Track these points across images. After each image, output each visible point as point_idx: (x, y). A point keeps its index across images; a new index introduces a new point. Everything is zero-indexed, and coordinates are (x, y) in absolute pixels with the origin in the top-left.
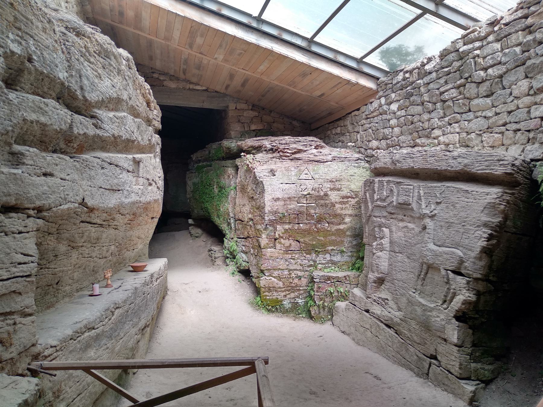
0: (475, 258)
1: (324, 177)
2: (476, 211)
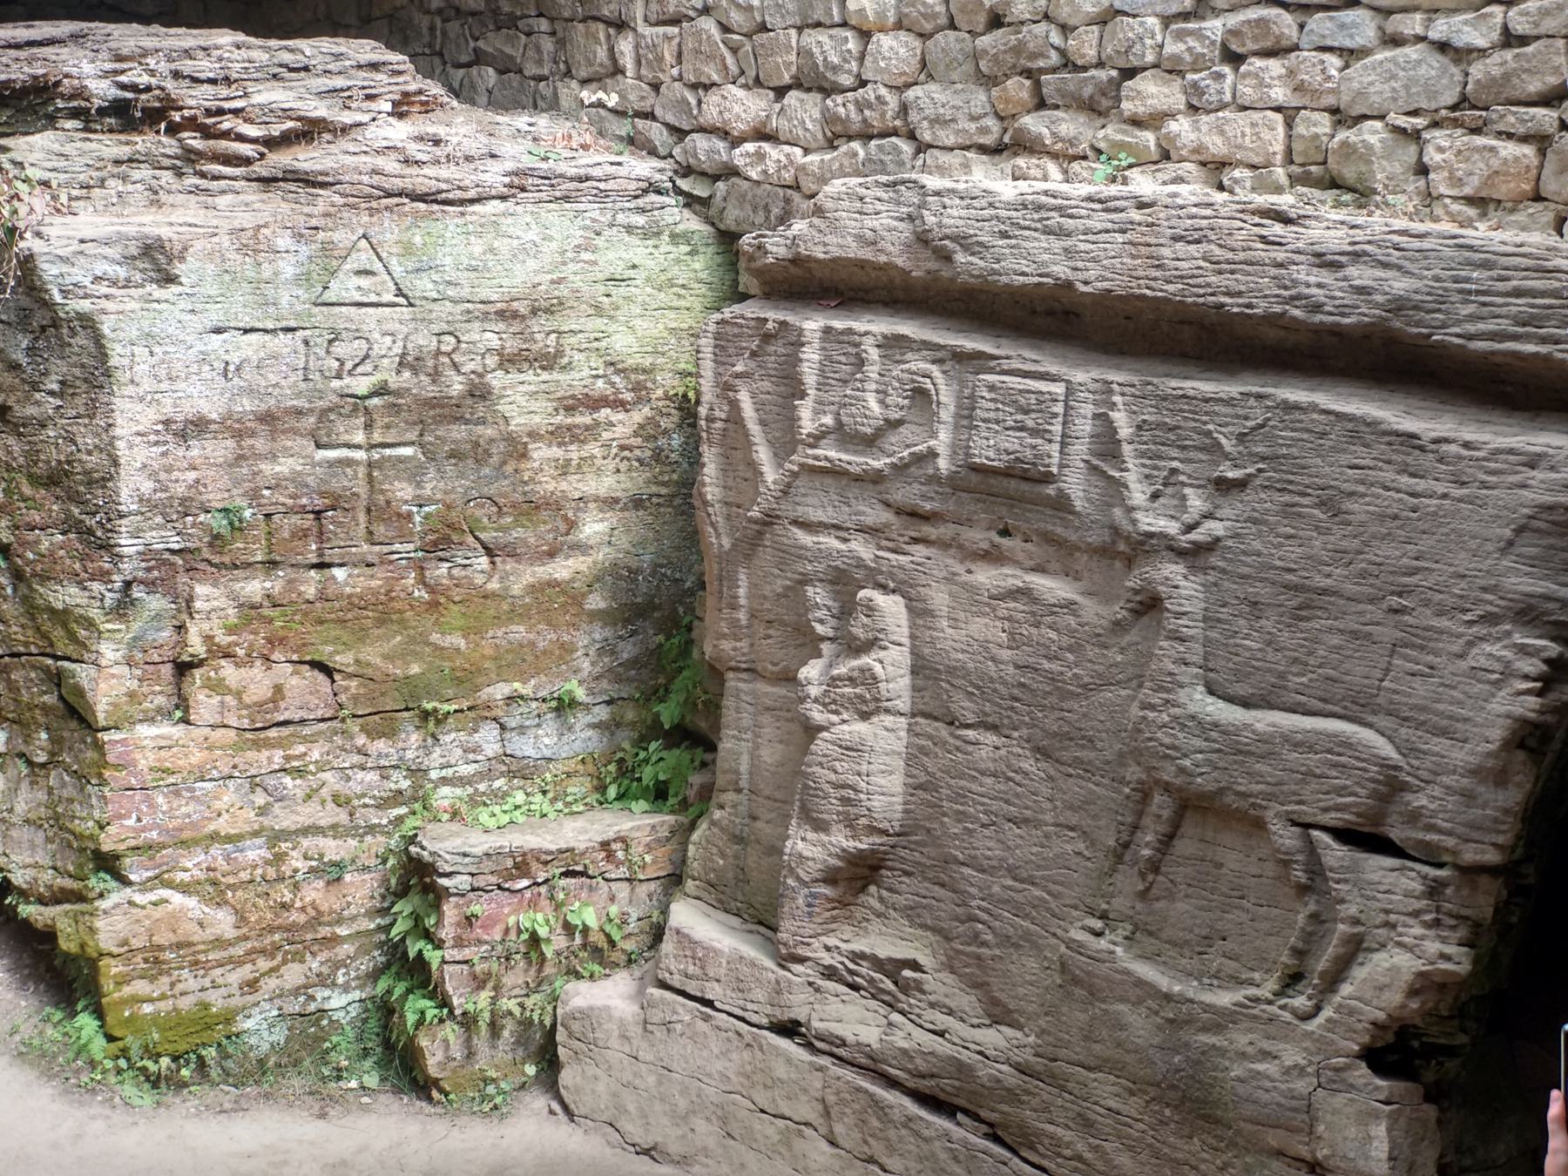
0: (1476, 772)
1: (465, 292)
2: (1473, 544)
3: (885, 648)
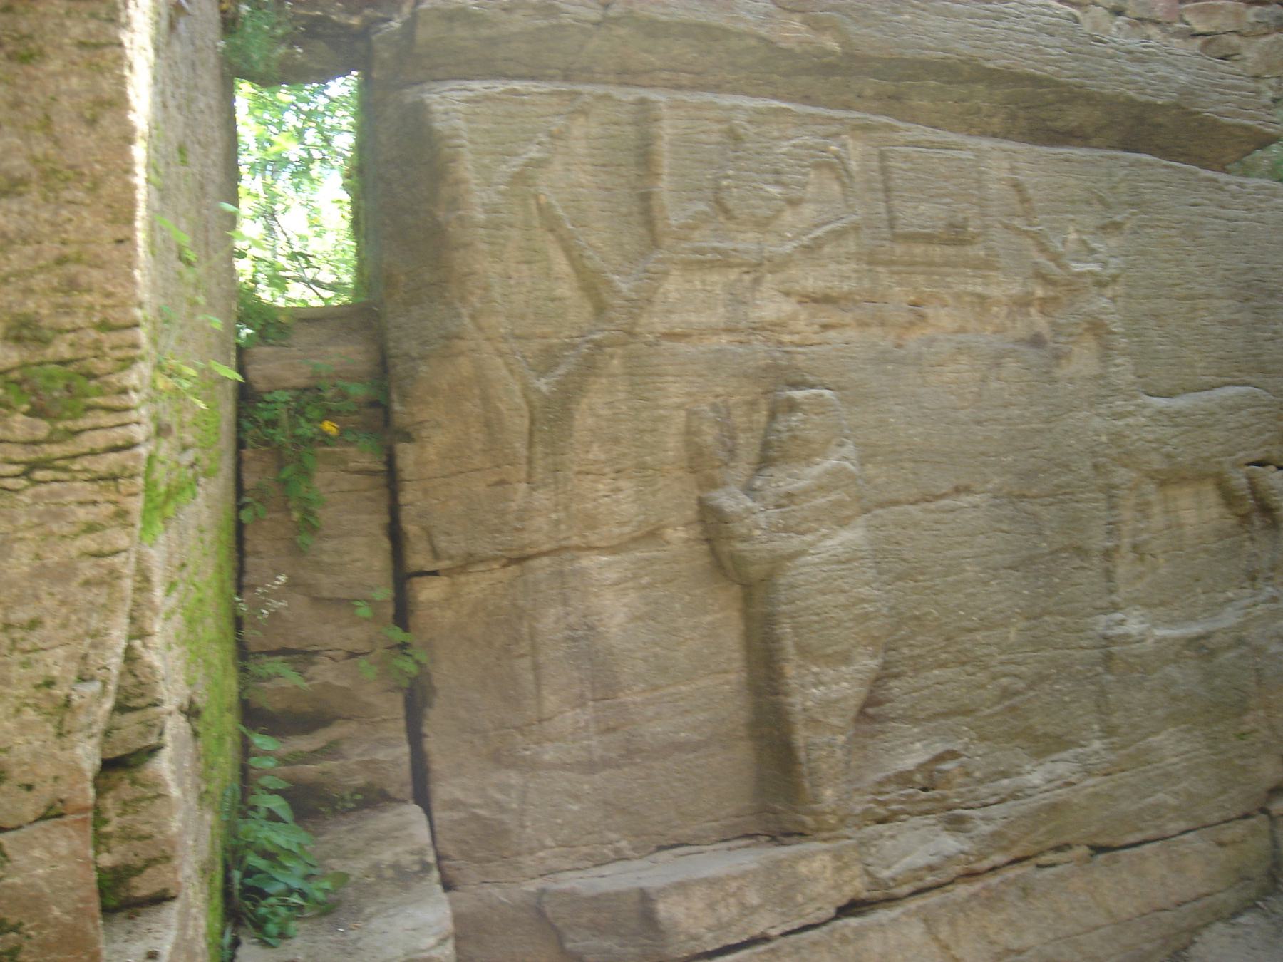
3: (841, 445)
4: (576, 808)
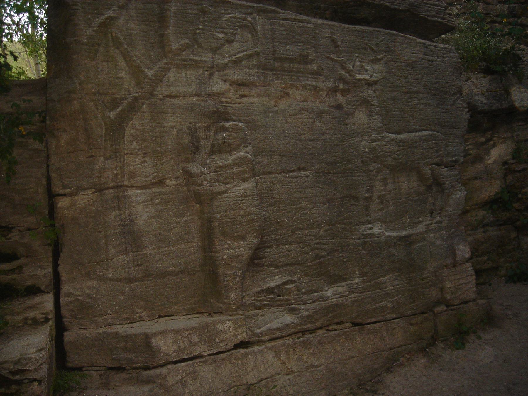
3: (246, 147)
4: (122, 298)
